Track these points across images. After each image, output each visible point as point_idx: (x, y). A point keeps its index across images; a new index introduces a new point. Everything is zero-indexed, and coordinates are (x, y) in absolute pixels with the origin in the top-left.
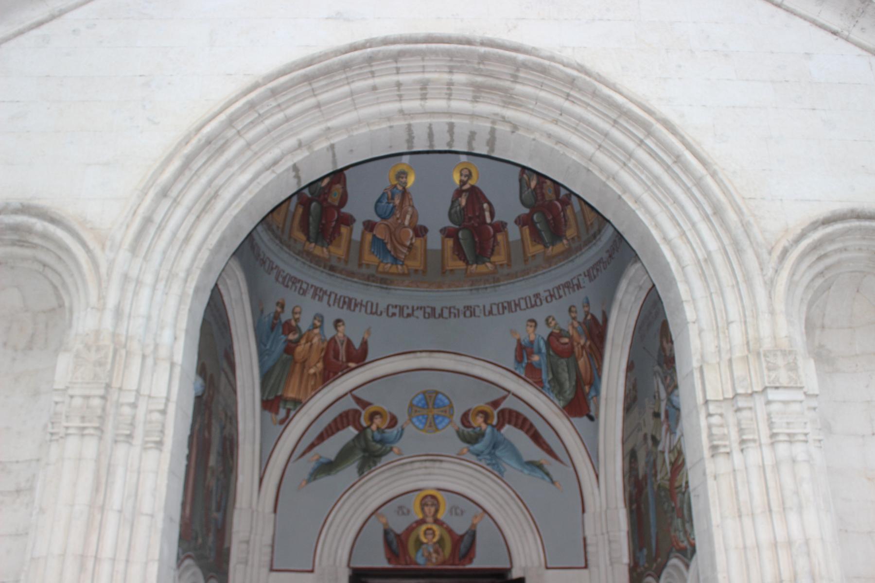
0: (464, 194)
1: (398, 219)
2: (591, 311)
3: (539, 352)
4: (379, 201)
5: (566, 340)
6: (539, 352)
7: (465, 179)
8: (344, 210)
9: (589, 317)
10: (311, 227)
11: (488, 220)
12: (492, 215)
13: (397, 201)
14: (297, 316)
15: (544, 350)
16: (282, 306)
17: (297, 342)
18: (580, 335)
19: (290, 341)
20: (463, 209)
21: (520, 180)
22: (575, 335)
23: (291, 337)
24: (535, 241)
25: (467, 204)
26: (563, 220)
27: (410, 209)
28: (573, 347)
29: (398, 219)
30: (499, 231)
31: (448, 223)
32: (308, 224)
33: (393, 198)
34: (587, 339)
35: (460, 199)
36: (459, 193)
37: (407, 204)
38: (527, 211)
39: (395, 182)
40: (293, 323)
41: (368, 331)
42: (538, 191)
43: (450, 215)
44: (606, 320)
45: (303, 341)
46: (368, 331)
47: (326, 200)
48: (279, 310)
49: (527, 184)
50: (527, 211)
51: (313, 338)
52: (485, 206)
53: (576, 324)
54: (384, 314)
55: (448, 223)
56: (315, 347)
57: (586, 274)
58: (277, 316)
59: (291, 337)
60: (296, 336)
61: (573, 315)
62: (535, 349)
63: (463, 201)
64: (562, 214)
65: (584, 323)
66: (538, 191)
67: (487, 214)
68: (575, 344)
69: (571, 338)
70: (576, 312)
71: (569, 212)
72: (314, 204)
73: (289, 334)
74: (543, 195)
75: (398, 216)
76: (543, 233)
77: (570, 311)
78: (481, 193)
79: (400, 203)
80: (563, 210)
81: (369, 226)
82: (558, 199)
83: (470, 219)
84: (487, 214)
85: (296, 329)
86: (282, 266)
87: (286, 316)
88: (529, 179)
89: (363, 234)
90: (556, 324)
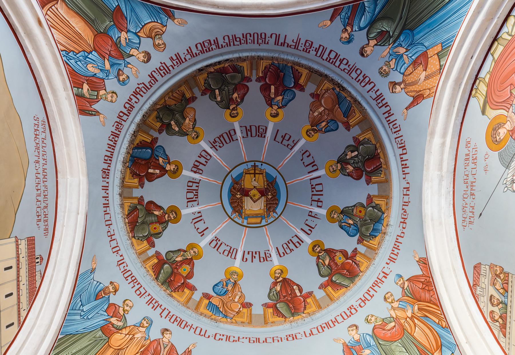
0: (279, 284)
1: (229, 297)
2: (405, 279)
3: (369, 346)
4: (216, 285)
5: (393, 324)
6: (369, 346)
7: (278, 276)
8: (188, 281)
9: (406, 284)
10: (161, 275)
11: (298, 294)
12: (301, 290)
13: (230, 288)
14: (127, 308)
15: (372, 342)
16: (116, 291)
17: (119, 329)
18: (404, 310)
19: (113, 325)
20: (279, 292)
21: (317, 265)
22: (400, 313)
23: (114, 320)
24: (338, 290)
25: (281, 289)
26: (355, 265)
27: (239, 293)
28: (401, 325)
29: (229, 297)
30: (308, 297)
31: (268, 301)
32: (159, 273)
33: (227, 286)
34: (413, 306)
35: (276, 287)
36: (275, 284)
37: (237, 290)
38: (327, 278)
39: (229, 277)
40: (122, 312)
41: (194, 345)
42: (332, 264)
43: (269, 296)
44: (424, 263)
45: (124, 331)
46: (194, 345)
47: (178, 269)
48: (111, 290)
49: (322, 264)
50: (327, 278)
51: (136, 333)
52: (295, 287)
53: (395, 305)
54: (212, 338)
55: (268, 301)
56: (135, 341)
57: (388, 261)
58: (105, 290)
59: (114, 320)
60: (120, 324)
61: (390, 300)
62: (364, 344)
63: (278, 288)
64: (353, 263)
65: (404, 294)
66: (332, 264)
67: (297, 292)
68: (402, 321)
69: (396, 320)
70: (392, 295)
71: (358, 258)
72: (166, 266)
73: (112, 317)
74: (336, 264)
75: (230, 296)
76: (342, 283)
77: (385, 299)
78: (291, 280)
79: (232, 289)
80: (353, 261)
81: (207, 296)
82: (347, 259)
83: (284, 297)
84: (297, 292)
85: (123, 318)
86: (126, 260)
87: (114, 299)
88: (323, 261)
89: (201, 298)
90: (376, 319)
